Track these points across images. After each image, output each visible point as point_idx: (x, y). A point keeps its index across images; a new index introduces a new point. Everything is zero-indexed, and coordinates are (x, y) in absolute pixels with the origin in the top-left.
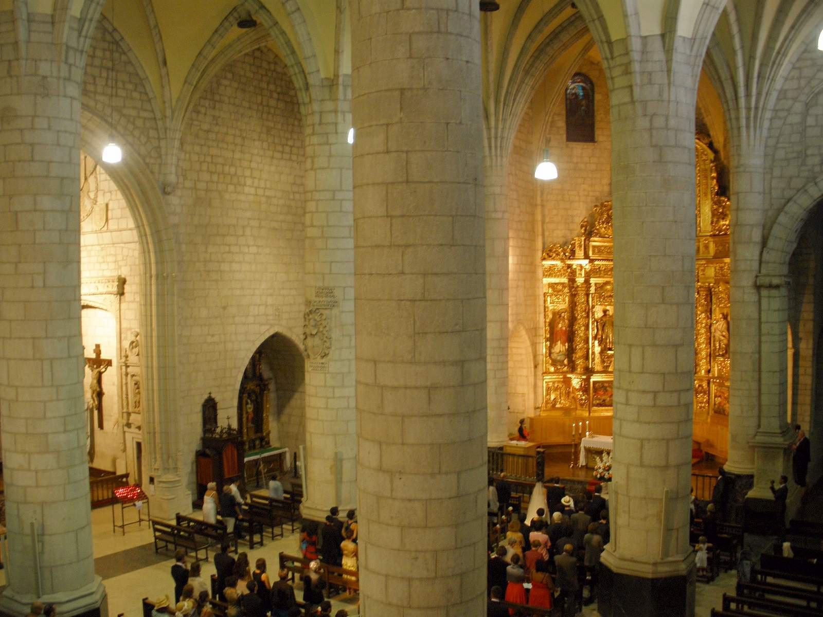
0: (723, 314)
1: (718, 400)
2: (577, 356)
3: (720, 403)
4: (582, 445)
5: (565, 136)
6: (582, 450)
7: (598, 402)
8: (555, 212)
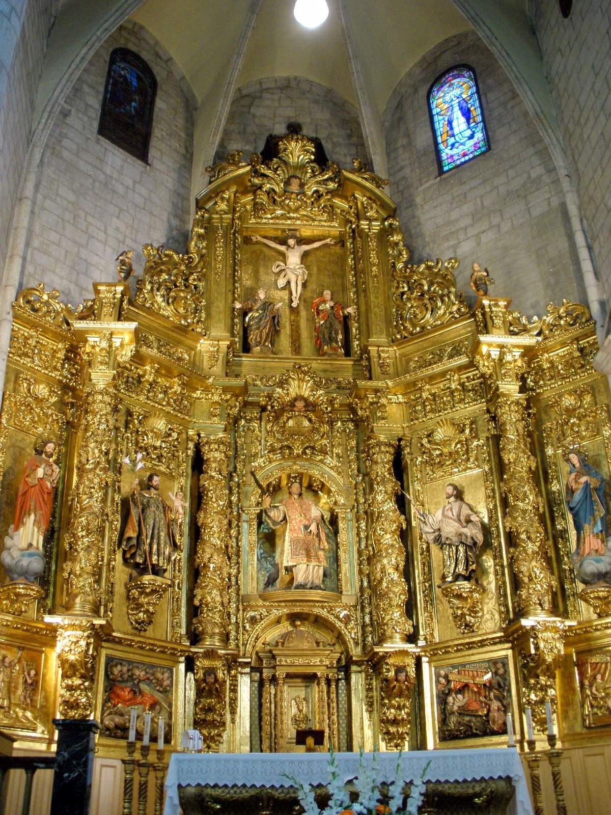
0: (455, 488)
1: (456, 702)
4: (171, 781)
5: (96, 124)
6: (172, 794)
7: (118, 719)
8: (54, 236)
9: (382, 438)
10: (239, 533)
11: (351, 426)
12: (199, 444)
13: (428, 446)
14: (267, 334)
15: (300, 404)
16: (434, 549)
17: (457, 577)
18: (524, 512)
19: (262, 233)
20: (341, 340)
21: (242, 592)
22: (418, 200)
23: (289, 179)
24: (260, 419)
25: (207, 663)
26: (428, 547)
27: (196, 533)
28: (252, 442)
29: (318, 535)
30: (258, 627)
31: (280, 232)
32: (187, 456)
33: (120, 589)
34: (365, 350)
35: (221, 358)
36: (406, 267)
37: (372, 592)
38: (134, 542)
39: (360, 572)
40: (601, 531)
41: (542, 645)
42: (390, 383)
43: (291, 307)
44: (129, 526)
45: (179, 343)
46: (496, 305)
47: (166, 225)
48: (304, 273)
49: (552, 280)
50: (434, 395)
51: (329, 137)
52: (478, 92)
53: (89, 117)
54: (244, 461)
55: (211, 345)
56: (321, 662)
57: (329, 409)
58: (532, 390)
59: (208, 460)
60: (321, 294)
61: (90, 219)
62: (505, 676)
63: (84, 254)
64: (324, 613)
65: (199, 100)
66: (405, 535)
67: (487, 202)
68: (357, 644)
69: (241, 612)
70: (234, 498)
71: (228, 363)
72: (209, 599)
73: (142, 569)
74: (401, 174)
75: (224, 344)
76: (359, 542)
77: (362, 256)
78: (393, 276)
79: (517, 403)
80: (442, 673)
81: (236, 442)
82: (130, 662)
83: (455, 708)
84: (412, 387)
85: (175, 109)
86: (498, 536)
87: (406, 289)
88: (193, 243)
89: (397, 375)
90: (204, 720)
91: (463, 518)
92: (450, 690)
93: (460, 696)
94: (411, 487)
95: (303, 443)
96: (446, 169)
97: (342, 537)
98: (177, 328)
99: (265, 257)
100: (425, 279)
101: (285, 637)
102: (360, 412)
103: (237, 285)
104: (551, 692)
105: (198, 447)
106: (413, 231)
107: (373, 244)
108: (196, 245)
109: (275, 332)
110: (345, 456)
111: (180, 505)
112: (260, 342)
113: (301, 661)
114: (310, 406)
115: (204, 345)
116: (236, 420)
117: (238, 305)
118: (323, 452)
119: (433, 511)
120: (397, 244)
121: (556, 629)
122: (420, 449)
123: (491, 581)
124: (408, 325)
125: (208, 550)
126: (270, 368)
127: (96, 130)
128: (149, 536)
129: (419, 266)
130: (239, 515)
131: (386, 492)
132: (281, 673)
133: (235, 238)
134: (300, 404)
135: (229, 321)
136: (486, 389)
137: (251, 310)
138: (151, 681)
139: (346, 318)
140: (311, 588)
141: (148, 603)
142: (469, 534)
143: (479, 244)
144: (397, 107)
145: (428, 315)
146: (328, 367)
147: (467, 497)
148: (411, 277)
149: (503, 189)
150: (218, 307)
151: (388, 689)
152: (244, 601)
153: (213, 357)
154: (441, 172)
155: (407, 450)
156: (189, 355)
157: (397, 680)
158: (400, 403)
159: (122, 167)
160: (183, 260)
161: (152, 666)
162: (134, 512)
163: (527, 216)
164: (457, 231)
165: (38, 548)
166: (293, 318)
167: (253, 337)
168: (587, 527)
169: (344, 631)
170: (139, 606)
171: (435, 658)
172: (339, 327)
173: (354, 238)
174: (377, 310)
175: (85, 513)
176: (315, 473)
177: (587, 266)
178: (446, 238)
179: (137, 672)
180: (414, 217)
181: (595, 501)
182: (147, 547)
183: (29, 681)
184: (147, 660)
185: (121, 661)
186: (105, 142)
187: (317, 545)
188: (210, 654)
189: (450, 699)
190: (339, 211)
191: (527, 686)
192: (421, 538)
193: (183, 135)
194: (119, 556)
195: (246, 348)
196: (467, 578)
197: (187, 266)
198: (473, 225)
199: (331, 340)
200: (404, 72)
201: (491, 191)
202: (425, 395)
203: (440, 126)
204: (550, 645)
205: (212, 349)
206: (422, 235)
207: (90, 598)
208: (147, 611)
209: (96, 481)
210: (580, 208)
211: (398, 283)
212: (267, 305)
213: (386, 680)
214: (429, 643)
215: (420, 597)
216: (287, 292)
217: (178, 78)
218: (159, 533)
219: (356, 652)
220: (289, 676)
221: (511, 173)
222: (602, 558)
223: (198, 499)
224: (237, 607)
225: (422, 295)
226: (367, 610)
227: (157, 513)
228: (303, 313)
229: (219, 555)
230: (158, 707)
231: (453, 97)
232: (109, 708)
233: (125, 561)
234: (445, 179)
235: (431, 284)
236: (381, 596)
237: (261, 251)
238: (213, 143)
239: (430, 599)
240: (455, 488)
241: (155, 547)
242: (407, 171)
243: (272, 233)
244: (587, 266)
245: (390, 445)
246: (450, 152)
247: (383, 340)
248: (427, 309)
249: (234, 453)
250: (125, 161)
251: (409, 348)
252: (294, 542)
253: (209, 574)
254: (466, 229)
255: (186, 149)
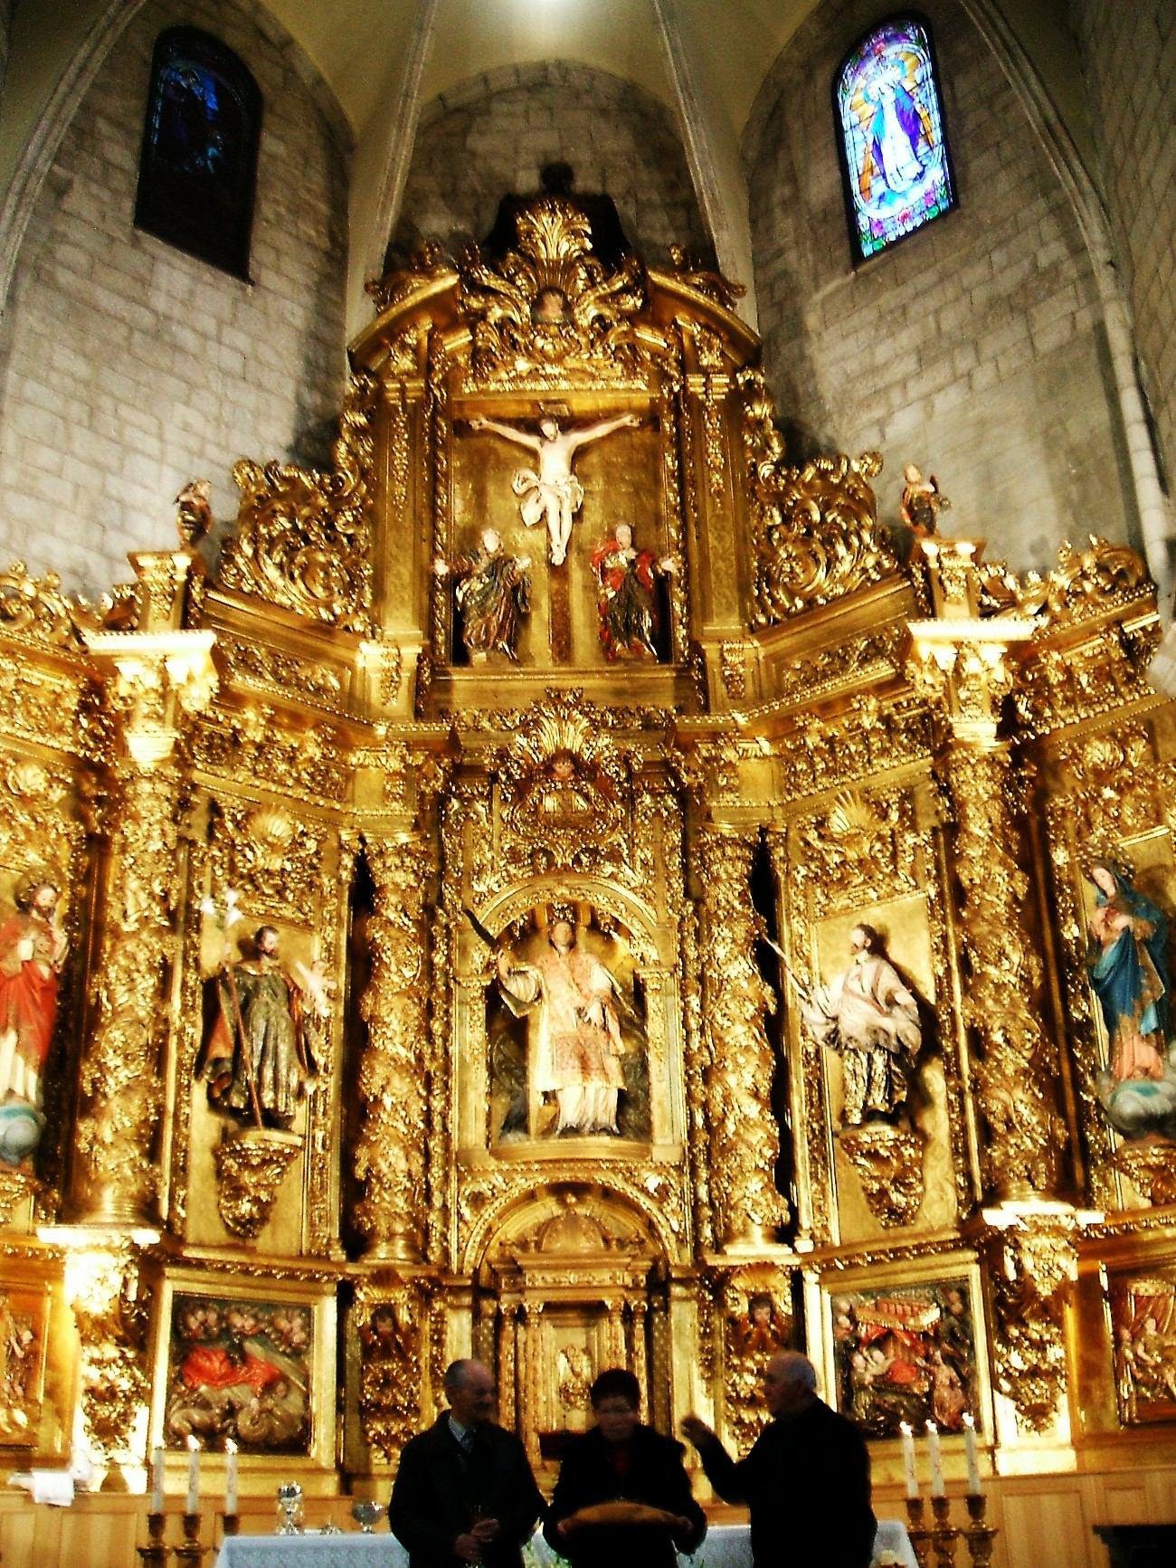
0: (869, 931)
1: (871, 1365)
2: (108, 1136)
3: (884, 1383)
5: (128, 206)
8: (47, 457)
9: (726, 828)
10: (448, 1025)
11: (671, 802)
12: (364, 856)
13: (818, 844)
14: (501, 626)
15: (563, 768)
16: (829, 1055)
17: (870, 1115)
18: (999, 987)
19: (493, 411)
20: (651, 630)
21: (455, 1146)
22: (812, 321)
23: (541, 295)
24: (489, 797)
25: (377, 1294)
26: (818, 1051)
27: (358, 1037)
28: (476, 844)
29: (605, 1027)
30: (489, 1212)
31: (528, 408)
32: (339, 882)
33: (201, 1161)
34: (696, 648)
35: (405, 681)
36: (777, 472)
37: (708, 1144)
38: (228, 1066)
39: (690, 1097)
40: (1156, 1031)
41: (1028, 1262)
42: (742, 720)
43: (551, 565)
44: (218, 1036)
45: (318, 655)
46: (953, 554)
47: (292, 408)
48: (574, 494)
49: (1074, 491)
50: (830, 741)
51: (630, 192)
52: (935, 75)
53: (115, 192)
54: (458, 881)
55: (383, 656)
56: (613, 1281)
57: (623, 775)
58: (1029, 727)
59: (383, 887)
60: (612, 534)
61: (124, 411)
62: (964, 1318)
63: (115, 485)
64: (618, 1183)
65: (356, 129)
66: (775, 1026)
67: (949, 323)
68: (681, 1241)
69: (454, 1185)
70: (439, 959)
71: (418, 688)
72: (385, 1169)
73: (246, 1118)
74: (778, 265)
75: (411, 652)
76: (687, 1039)
77: (692, 451)
78: (754, 493)
79: (992, 761)
80: (844, 1306)
81: (441, 843)
82: (223, 1302)
83: (868, 1379)
84: (783, 728)
85: (305, 155)
86: (954, 1031)
87: (778, 520)
88: (343, 448)
89: (760, 698)
90: (377, 1405)
91: (881, 997)
92: (858, 1341)
93: (877, 1354)
94: (785, 929)
95: (574, 842)
96: (867, 250)
97: (654, 1027)
98: (312, 628)
99: (498, 460)
100: (815, 499)
101: (544, 1229)
102: (685, 779)
103: (441, 525)
104: (1054, 1353)
105: (362, 864)
106: (801, 390)
107: (713, 424)
108: (350, 452)
109: (518, 619)
110: (660, 865)
111: (321, 987)
112: (486, 644)
113: (572, 1277)
114: (585, 769)
115: (370, 657)
116: (441, 800)
117: (441, 568)
118: (615, 856)
119: (827, 976)
120: (760, 423)
121: (1058, 1231)
122: (804, 853)
123: (938, 1122)
124: (781, 596)
125: (381, 1070)
126: (510, 692)
127: (129, 220)
128: (258, 1052)
129: (802, 471)
130: (449, 991)
131: (734, 941)
132: (533, 1303)
133: (434, 424)
134: (563, 768)
135: (426, 600)
136: (931, 732)
137: (468, 575)
138: (268, 1335)
139: (663, 581)
140: (592, 1133)
141: (257, 1185)
142: (892, 1031)
143: (929, 416)
144: (771, 116)
145: (821, 574)
146: (626, 684)
147: (894, 951)
148: (787, 493)
149: (980, 295)
150: (398, 576)
151: (740, 1338)
152: (459, 1161)
153: (390, 681)
154: (857, 258)
155: (780, 852)
156: (340, 680)
157: (753, 1320)
158: (765, 757)
159: (192, 293)
160: (321, 485)
161: (270, 1306)
162: (227, 1007)
163: (1028, 353)
164: (887, 388)
165: (26, 1098)
166: (555, 586)
167: (473, 628)
168: (1125, 1020)
169: (657, 1217)
170: (237, 1191)
171: (831, 1276)
172: (642, 600)
173: (678, 414)
174: (721, 564)
175: (121, 1022)
176: (602, 904)
177: (1143, 464)
178: (866, 404)
179: (238, 1321)
180: (803, 357)
181: (1146, 968)
182: (252, 1077)
183: (20, 1353)
184: (261, 1294)
185: (203, 1302)
186: (153, 244)
187: (603, 1046)
188: (384, 1277)
189: (858, 1360)
190: (648, 356)
191: (1006, 1341)
192: (804, 1034)
193: (323, 208)
194: (199, 1092)
195: (460, 656)
196: (890, 1119)
197: (330, 496)
198: (918, 375)
199: (631, 629)
200: (784, 36)
201: (957, 299)
202: (812, 741)
203: (858, 156)
204: (1049, 1263)
205: (387, 665)
206: (817, 398)
207: (134, 1189)
208: (256, 1201)
209: (142, 956)
210: (1134, 335)
211: (762, 508)
212: (500, 564)
213: (732, 1320)
214: (822, 1247)
215: (802, 1151)
216: (544, 531)
217: (308, 81)
218: (276, 1047)
219: (680, 1258)
220: (550, 1307)
221: (998, 257)
222: (1156, 1085)
223: (362, 965)
224: (446, 1176)
225: (809, 534)
226: (704, 1174)
227: (273, 1006)
228: (577, 576)
229: (402, 1079)
230: (281, 1387)
231: (885, 87)
232: (181, 1395)
233: (214, 1105)
234: (866, 274)
235: (826, 507)
236: (727, 1150)
237: (493, 451)
238: (382, 228)
239: (819, 1155)
240: (869, 931)
241: (268, 1074)
242: (792, 256)
243: (512, 410)
244: (1143, 464)
245: (749, 845)
246: (876, 215)
247: (733, 624)
248: (817, 562)
249: (439, 872)
250: (196, 279)
251: (784, 643)
252: (558, 1040)
253: (384, 1116)
254: (903, 384)
255: (333, 238)
